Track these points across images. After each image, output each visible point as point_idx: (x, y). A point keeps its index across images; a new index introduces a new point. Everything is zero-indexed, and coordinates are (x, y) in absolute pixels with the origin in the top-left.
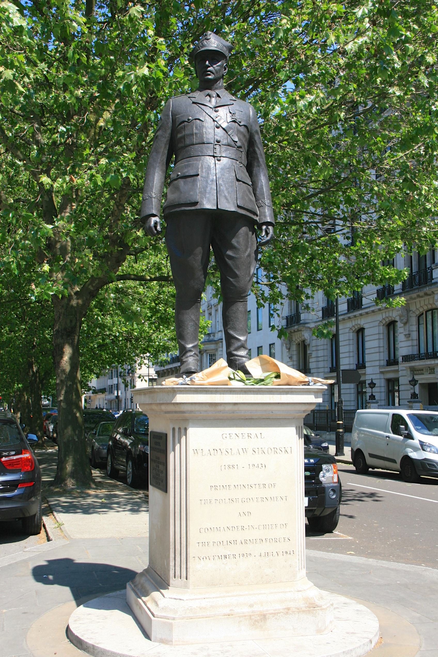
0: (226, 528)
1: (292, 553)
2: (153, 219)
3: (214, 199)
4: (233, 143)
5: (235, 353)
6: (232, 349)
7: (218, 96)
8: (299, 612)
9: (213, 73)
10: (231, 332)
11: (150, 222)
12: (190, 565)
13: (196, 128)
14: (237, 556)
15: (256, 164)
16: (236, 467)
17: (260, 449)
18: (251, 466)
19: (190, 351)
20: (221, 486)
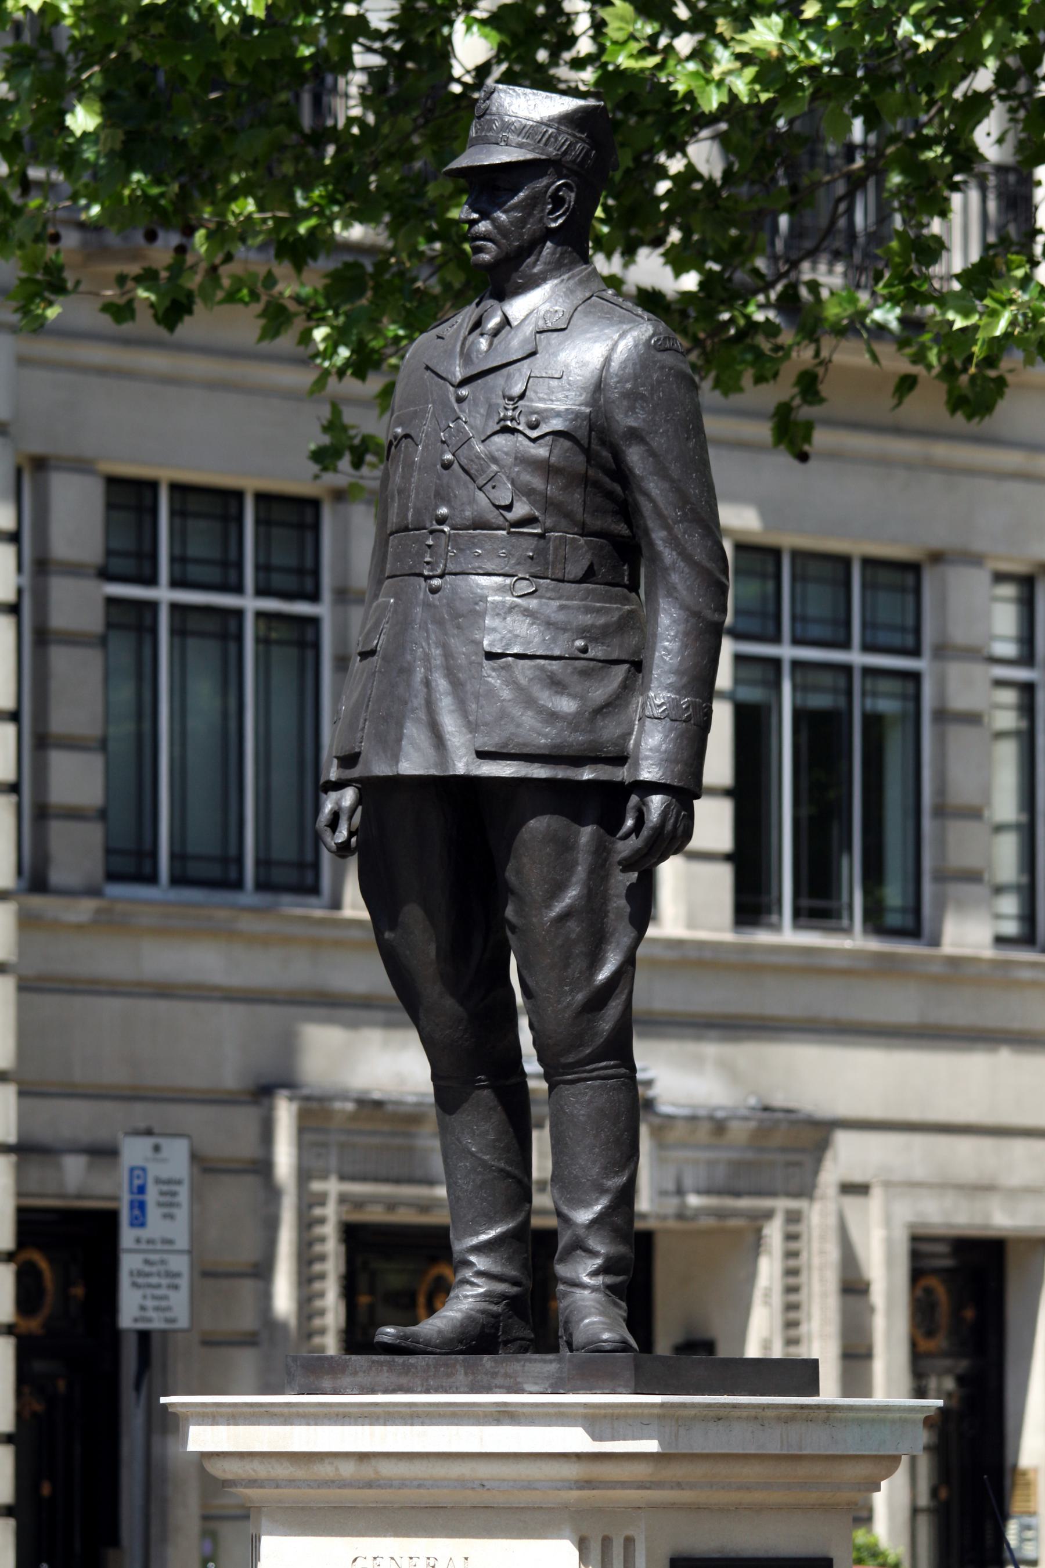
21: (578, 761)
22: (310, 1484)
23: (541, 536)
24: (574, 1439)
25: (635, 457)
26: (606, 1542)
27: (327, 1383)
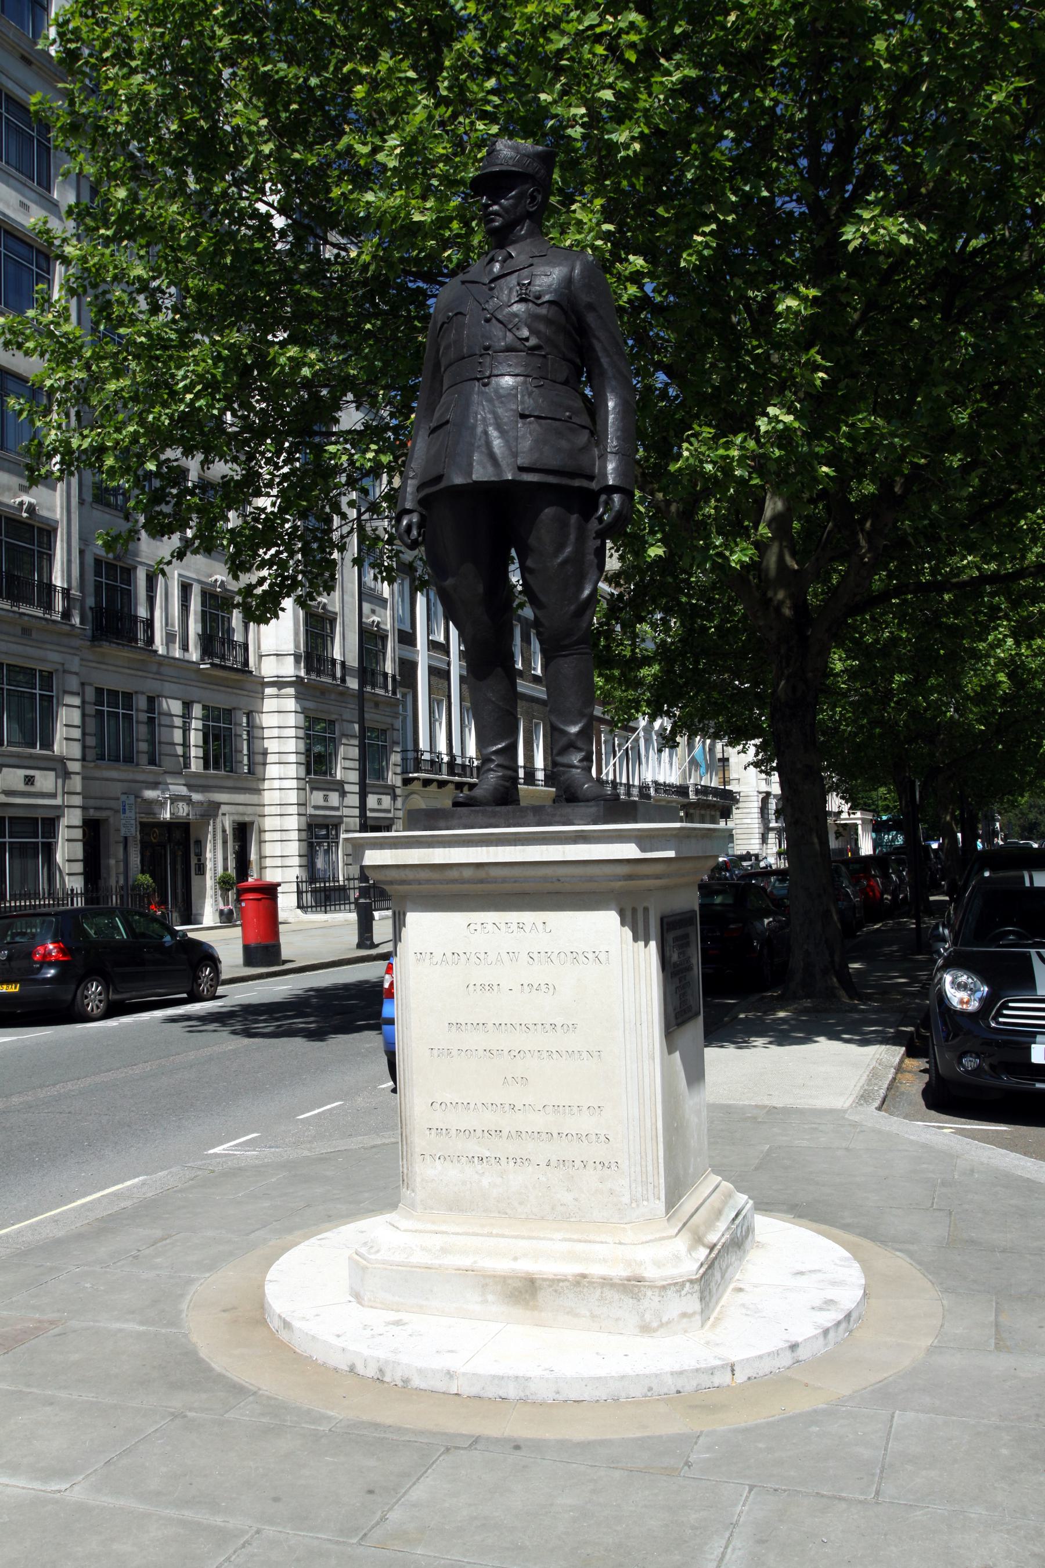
0: (479, 1105)
1: (613, 1166)
8: (603, 1285)
14: (503, 1160)
16: (495, 987)
21: (573, 475)
23: (544, 356)
24: (629, 851)
25: (591, 318)
26: (634, 911)
27: (442, 824)
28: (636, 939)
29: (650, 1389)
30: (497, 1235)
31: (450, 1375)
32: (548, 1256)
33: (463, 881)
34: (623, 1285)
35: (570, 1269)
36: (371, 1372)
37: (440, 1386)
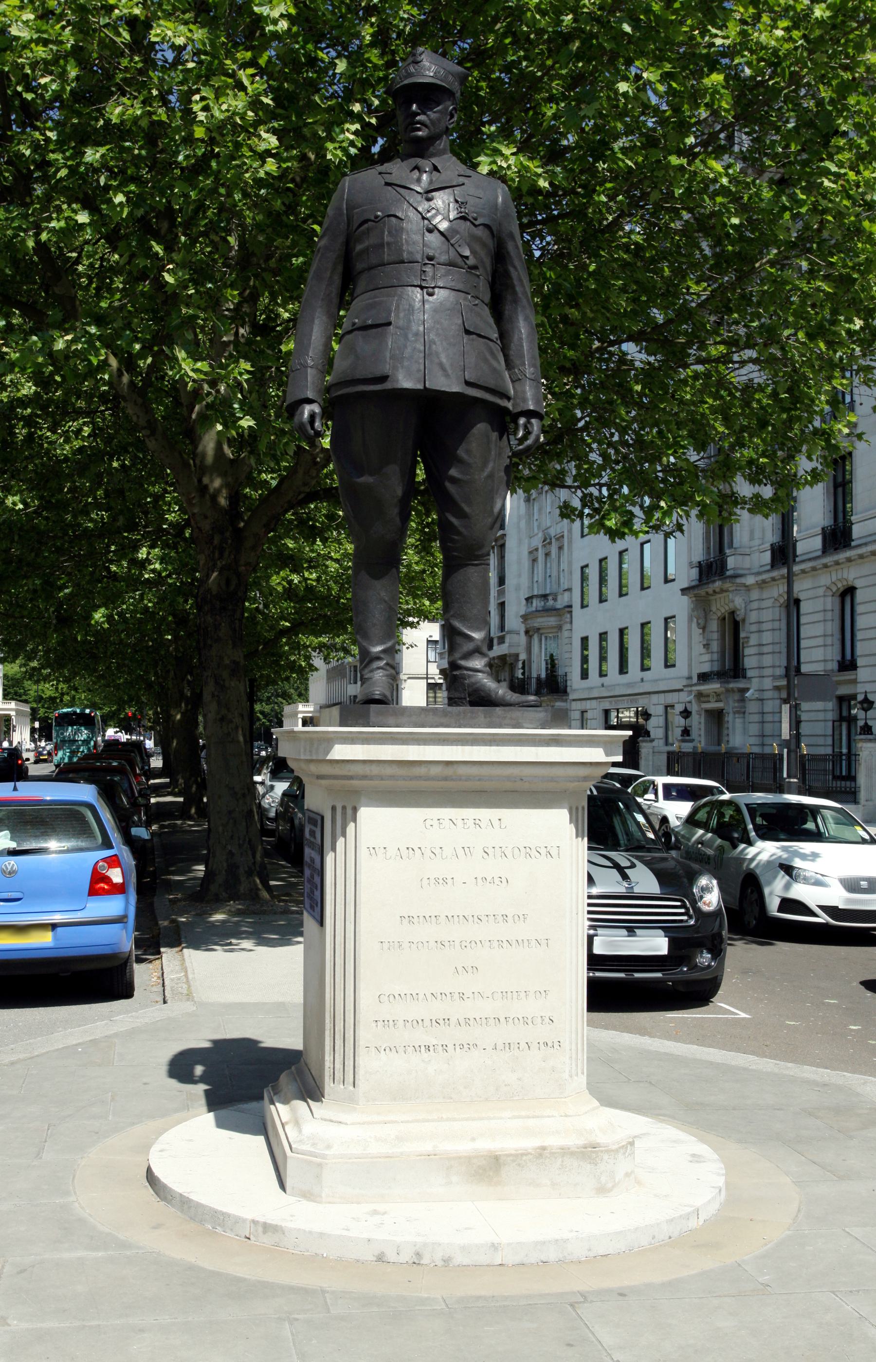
0: (429, 996)
1: (556, 1045)
2: (307, 409)
3: (419, 371)
4: (459, 261)
5: (463, 663)
6: (457, 655)
7: (435, 168)
9: (426, 126)
10: (457, 624)
11: (303, 413)
12: (360, 1061)
13: (389, 232)
14: (450, 1048)
15: (509, 297)
16: (449, 881)
17: (497, 848)
18: (479, 880)
19: (378, 658)
20: (421, 918)
22: (411, 779)
25: (510, 246)
26: (577, 809)
27: (391, 720)
28: (577, 836)
29: (654, 1238)
30: (448, 1120)
31: (495, 1247)
32: (506, 1134)
33: (428, 778)
34: (582, 1152)
35: (530, 1143)
36: (407, 1256)
37: (483, 1259)
